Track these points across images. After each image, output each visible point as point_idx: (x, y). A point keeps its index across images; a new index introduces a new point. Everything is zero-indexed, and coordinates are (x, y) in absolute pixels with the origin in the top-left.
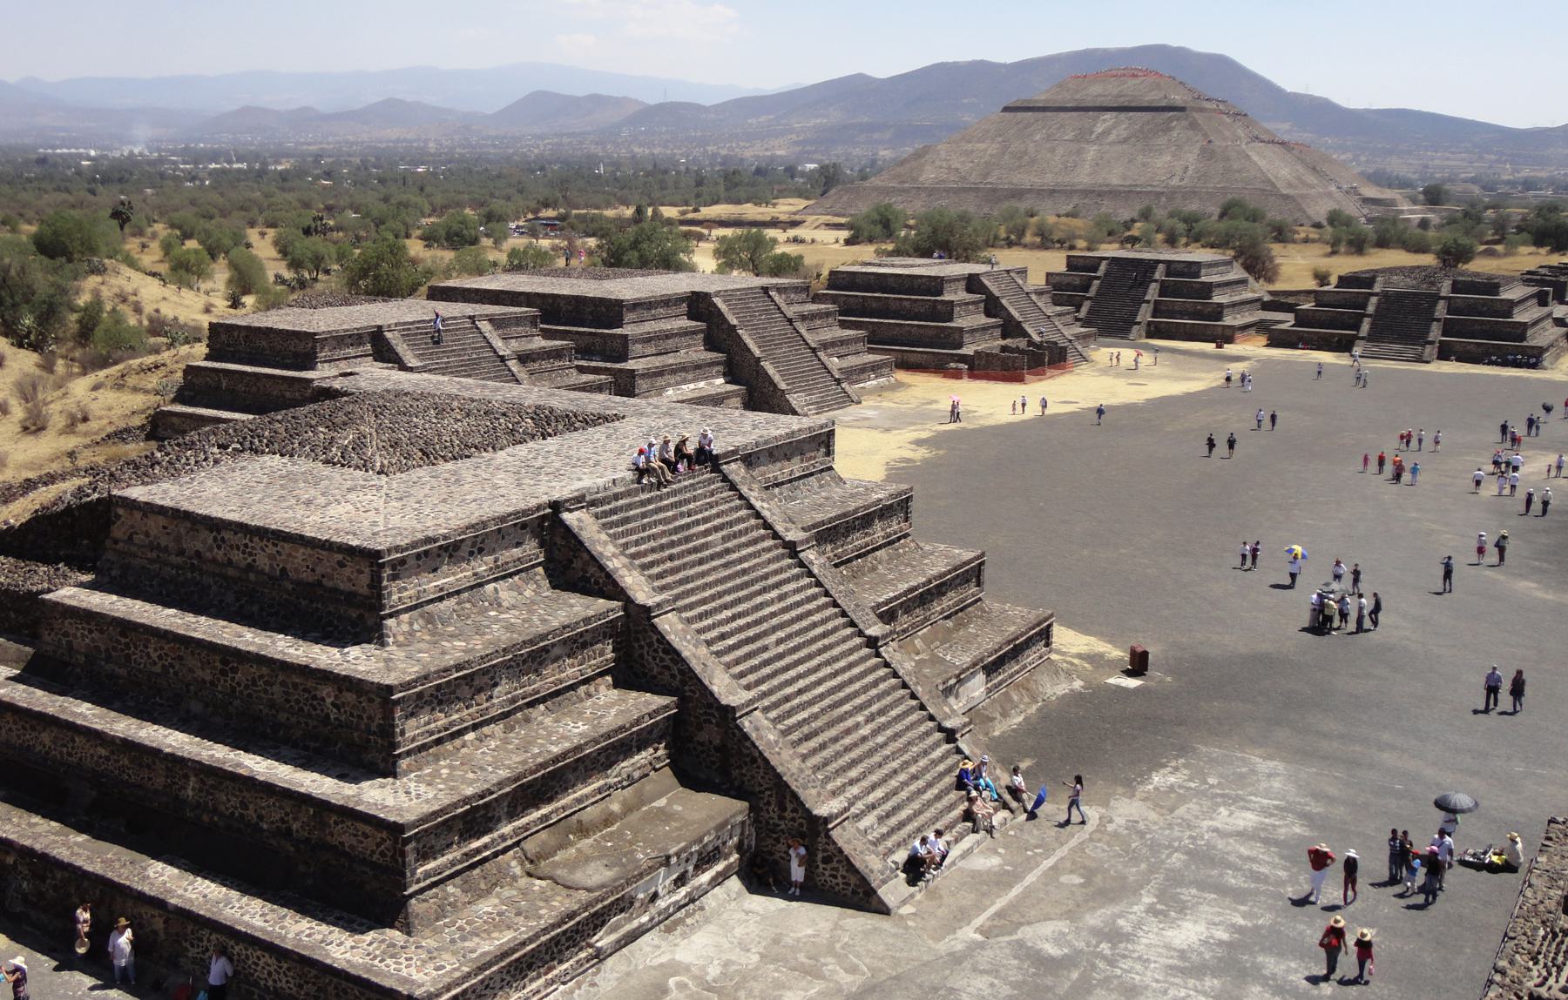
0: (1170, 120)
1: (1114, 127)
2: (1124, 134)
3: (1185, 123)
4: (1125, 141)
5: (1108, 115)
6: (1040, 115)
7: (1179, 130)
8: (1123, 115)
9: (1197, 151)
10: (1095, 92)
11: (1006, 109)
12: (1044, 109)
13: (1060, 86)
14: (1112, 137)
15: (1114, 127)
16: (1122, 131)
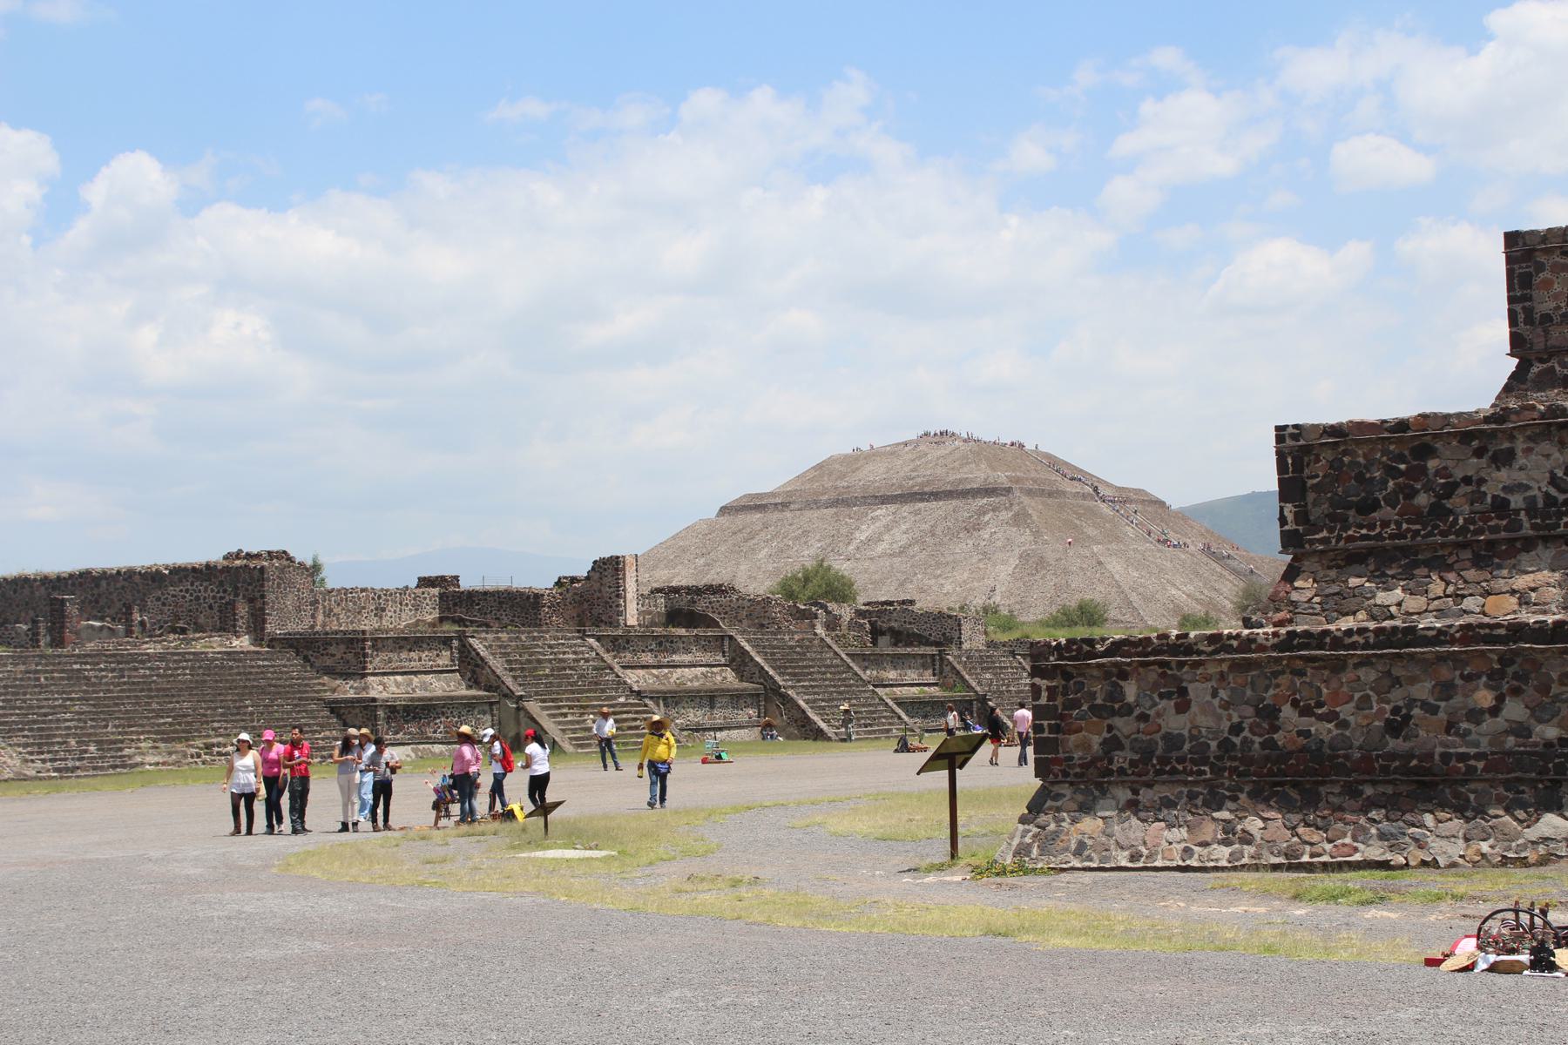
0: (982, 512)
1: (888, 528)
2: (904, 540)
3: (1005, 515)
4: (903, 551)
5: (881, 511)
6: (776, 516)
7: (996, 527)
8: (906, 509)
9: (1014, 561)
10: (874, 475)
11: (724, 510)
12: (785, 505)
13: (820, 467)
14: (881, 547)
15: (888, 528)
16: (900, 537)
